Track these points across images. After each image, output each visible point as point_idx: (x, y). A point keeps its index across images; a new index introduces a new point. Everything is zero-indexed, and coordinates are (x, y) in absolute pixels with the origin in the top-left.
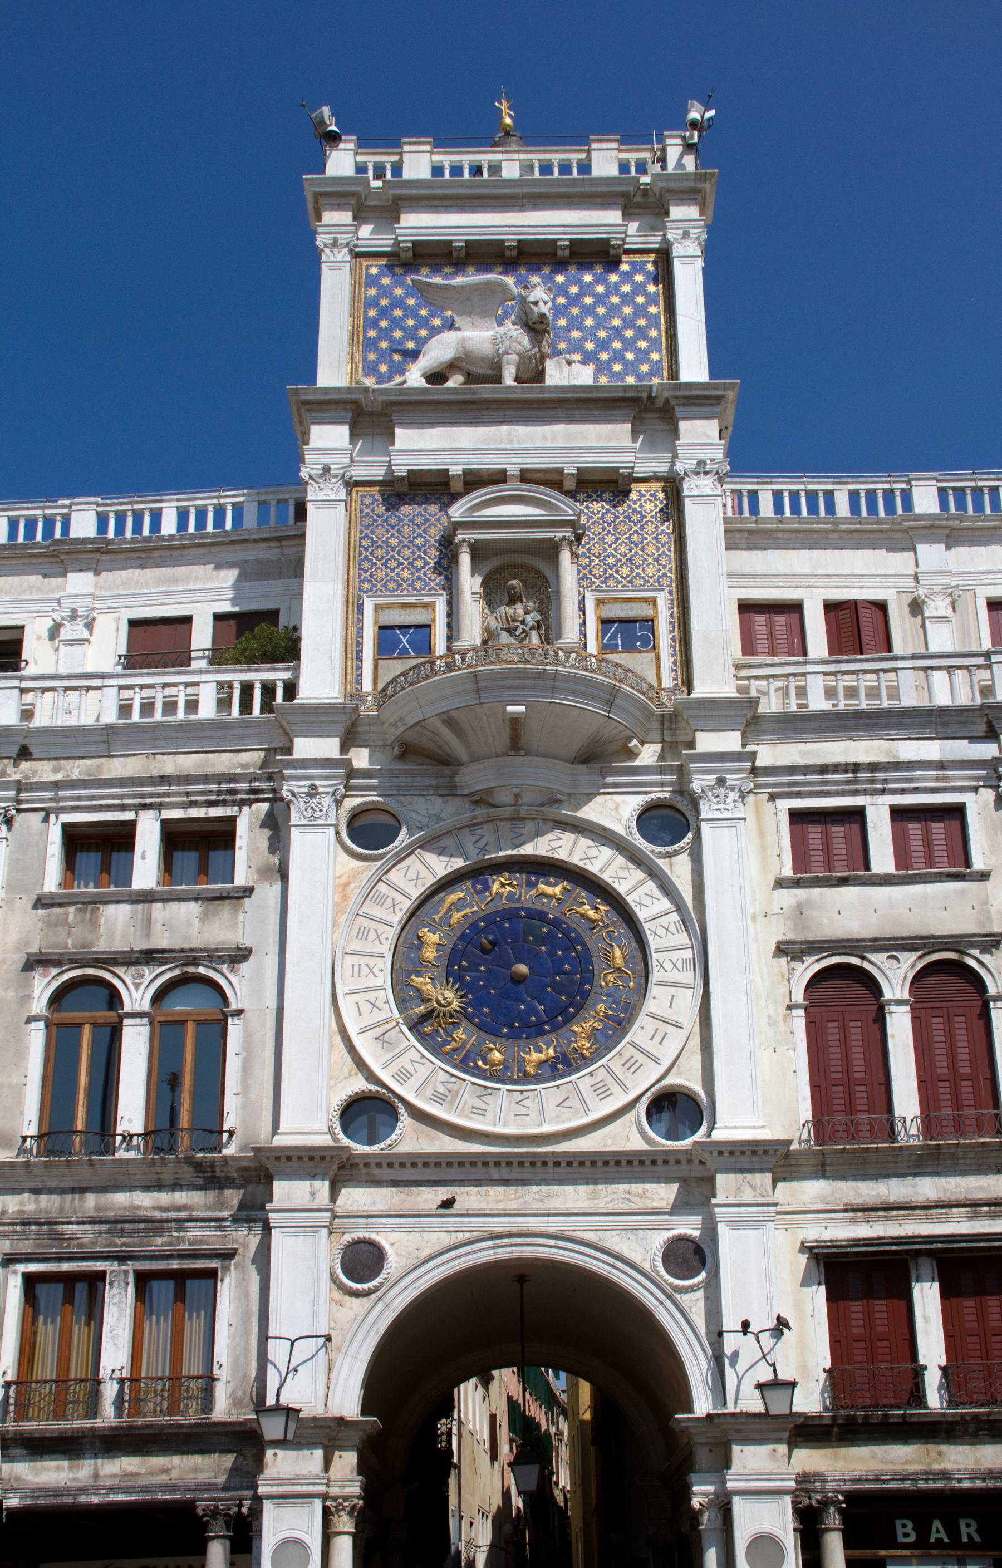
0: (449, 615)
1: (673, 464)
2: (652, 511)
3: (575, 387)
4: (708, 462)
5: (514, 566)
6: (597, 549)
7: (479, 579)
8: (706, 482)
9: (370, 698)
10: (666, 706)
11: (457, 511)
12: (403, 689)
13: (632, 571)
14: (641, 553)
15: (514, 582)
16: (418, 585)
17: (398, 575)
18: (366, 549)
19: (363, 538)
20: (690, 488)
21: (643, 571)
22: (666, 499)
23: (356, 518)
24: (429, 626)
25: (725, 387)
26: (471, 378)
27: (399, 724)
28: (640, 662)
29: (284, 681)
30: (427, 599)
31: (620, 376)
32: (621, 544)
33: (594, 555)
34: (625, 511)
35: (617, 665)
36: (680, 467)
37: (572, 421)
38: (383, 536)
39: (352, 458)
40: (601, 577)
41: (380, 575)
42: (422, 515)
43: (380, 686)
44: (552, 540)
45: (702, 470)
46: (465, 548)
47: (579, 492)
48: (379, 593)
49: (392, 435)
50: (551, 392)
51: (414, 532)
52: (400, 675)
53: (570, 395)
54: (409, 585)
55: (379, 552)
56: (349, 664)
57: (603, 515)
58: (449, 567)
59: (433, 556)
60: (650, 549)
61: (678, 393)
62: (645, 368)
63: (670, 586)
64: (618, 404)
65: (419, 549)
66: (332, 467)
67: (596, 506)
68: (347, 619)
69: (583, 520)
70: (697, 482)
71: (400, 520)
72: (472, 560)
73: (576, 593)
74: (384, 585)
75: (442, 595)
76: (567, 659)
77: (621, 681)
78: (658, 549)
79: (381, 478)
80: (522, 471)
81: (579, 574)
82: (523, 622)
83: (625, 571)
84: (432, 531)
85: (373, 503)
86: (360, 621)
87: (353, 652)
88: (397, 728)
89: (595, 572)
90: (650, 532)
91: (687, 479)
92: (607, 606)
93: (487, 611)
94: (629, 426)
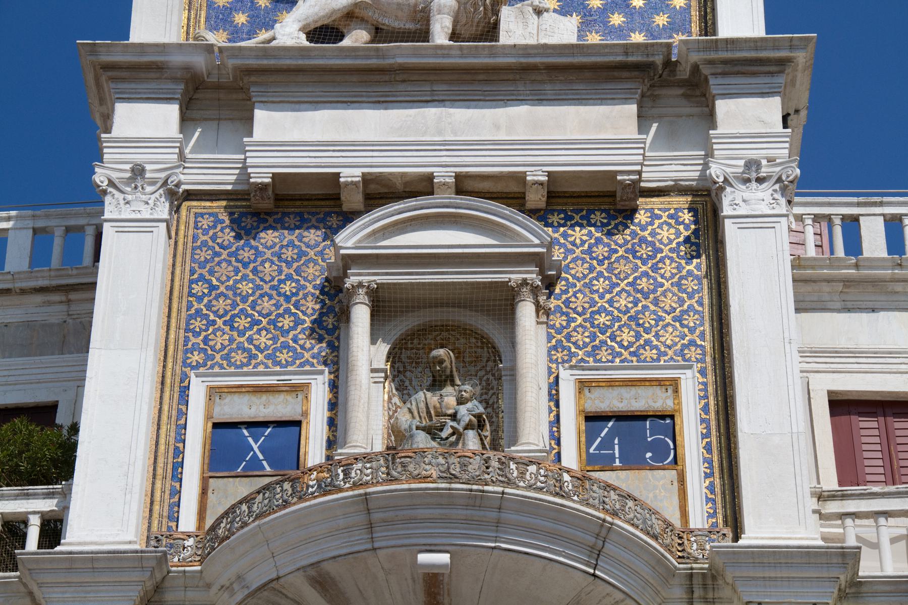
0: (333, 405)
1: (706, 166)
2: (671, 242)
3: (545, 46)
4: (764, 162)
5: (444, 327)
6: (580, 301)
7: (383, 349)
8: (760, 195)
9: (190, 542)
10: (696, 560)
11: (351, 238)
12: (245, 524)
13: (638, 336)
14: (652, 308)
15: (441, 352)
16: (283, 357)
17: (250, 340)
18: (200, 299)
19: (196, 282)
20: (734, 204)
21: (657, 336)
22: (696, 222)
23: (185, 249)
24: (298, 424)
25: (792, 45)
26: (379, 33)
27: (236, 586)
28: (652, 487)
29: (43, 515)
30: (297, 379)
31: (619, 31)
32: (619, 294)
33: (574, 310)
34: (626, 242)
35: (608, 487)
36: (716, 171)
37: (541, 100)
38: (229, 278)
39: (182, 156)
40: (585, 345)
41: (220, 340)
42: (294, 246)
43: (209, 522)
44: (505, 284)
45: (754, 175)
46: (362, 296)
47: (552, 212)
48: (217, 370)
49: (250, 119)
50: (506, 55)
51: (280, 272)
52: (240, 502)
53: (538, 60)
54: (268, 357)
55: (221, 305)
56: (158, 485)
57: (590, 247)
58: (336, 328)
59: (309, 311)
60: (669, 302)
61: (713, 55)
62: (661, 20)
63: (702, 361)
64: (616, 74)
65: (288, 299)
66: (148, 167)
67: (578, 234)
68: (160, 411)
69: (557, 254)
70: (746, 195)
71: (258, 253)
72: (372, 316)
73: (544, 371)
74: (227, 357)
75: (321, 373)
76: (522, 474)
77: (615, 514)
78: (681, 302)
79: (229, 187)
80: (458, 177)
81: (549, 341)
82: (454, 417)
83: (627, 336)
84: (311, 271)
85: (215, 227)
86: (182, 414)
87: (167, 466)
88: (233, 593)
89: (577, 337)
90: (668, 275)
91: (728, 189)
92: (597, 393)
93: (396, 400)
94: (634, 108)
